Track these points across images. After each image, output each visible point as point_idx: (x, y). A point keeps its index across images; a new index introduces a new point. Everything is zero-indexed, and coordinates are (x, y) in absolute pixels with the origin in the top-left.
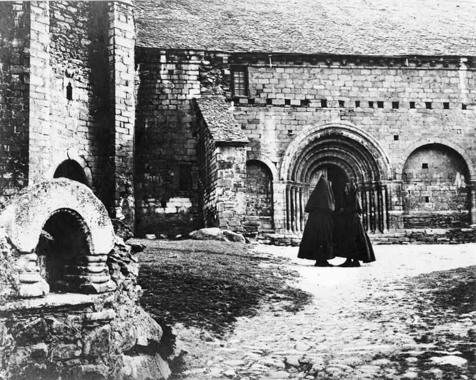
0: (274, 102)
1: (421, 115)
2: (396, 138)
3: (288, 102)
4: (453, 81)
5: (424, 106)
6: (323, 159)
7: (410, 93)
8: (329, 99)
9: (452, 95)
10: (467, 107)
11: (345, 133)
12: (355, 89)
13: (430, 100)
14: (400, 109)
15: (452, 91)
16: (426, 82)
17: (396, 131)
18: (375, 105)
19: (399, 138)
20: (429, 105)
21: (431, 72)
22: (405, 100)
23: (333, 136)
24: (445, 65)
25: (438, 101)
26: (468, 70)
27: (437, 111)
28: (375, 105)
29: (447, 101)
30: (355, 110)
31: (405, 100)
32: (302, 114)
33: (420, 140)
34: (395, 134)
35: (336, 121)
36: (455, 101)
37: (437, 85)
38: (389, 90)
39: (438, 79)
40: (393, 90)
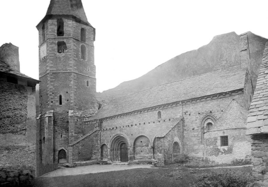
0: (108, 129)
3: (110, 129)
5: (139, 124)
6: (120, 143)
8: (117, 126)
11: (121, 135)
12: (123, 123)
14: (133, 127)
18: (127, 126)
22: (134, 124)
23: (119, 136)
28: (127, 126)
29: (144, 122)
30: (123, 128)
32: (113, 131)
35: (119, 133)
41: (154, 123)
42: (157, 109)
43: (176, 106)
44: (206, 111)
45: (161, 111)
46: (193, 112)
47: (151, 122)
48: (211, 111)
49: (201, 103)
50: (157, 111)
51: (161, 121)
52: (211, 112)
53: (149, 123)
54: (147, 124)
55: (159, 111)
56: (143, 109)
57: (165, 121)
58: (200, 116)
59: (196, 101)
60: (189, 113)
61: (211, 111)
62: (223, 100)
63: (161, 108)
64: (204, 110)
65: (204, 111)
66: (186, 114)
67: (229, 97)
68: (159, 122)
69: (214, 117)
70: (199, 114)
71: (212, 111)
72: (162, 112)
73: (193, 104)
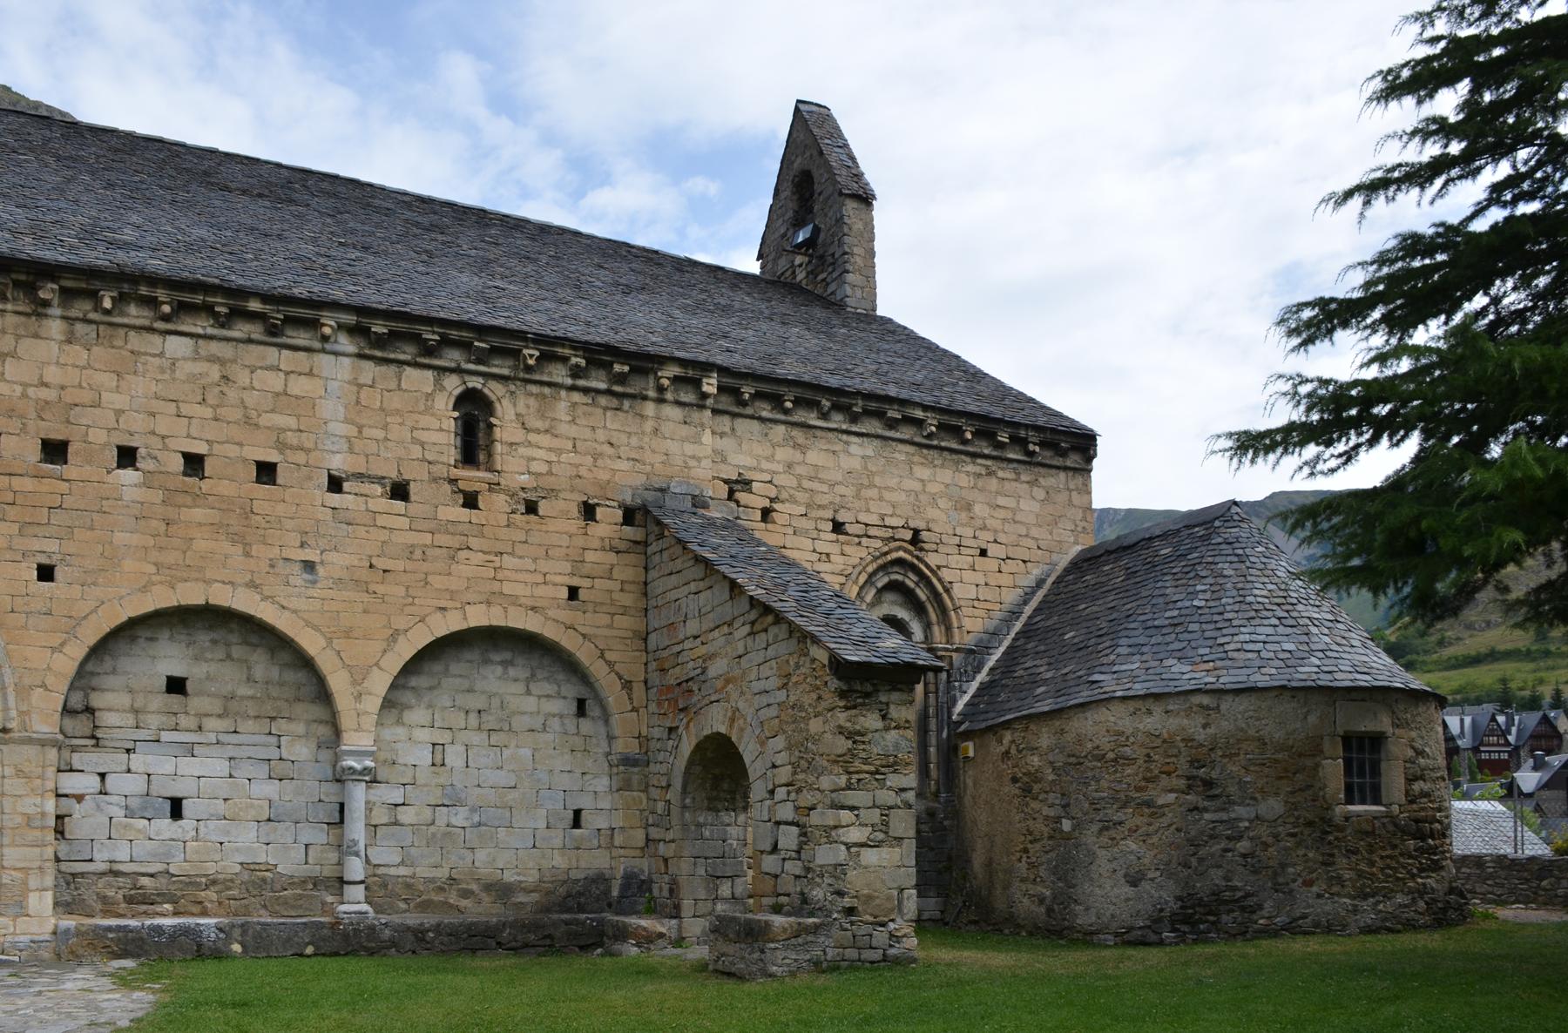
1: (158, 496)
2: (46, 573)
4: (299, 386)
5: (178, 463)
7: (119, 413)
9: (292, 438)
10: (346, 486)
13: (199, 448)
15: (292, 422)
16: (192, 378)
17: (48, 548)
19: (58, 573)
20: (194, 463)
21: (214, 347)
24: (273, 331)
25: (233, 451)
26: (361, 356)
27: (226, 488)
29: (272, 456)
31: (98, 436)
33: (144, 589)
34: (44, 560)
36: (300, 458)
37: (232, 394)
38: (31, 391)
39: (243, 378)
40: (44, 393)
41: (400, 491)
42: (453, 357)
43: (620, 397)
44: (888, 521)
45: (494, 390)
46: (795, 501)
47: (360, 477)
48: (916, 532)
49: (858, 448)
50: (454, 385)
51: (496, 506)
52: (916, 540)
53: (335, 484)
54: (302, 494)
55: (475, 383)
56: (266, 298)
57: (531, 508)
58: (847, 549)
59: (824, 416)
60: (767, 503)
61: (916, 532)
62: (989, 474)
63: (501, 367)
64: (873, 507)
65: (873, 519)
66: (742, 496)
67: (1021, 468)
68: (471, 501)
69: (935, 581)
70: (838, 527)
71: (924, 535)
72: (511, 411)
73: (798, 434)
